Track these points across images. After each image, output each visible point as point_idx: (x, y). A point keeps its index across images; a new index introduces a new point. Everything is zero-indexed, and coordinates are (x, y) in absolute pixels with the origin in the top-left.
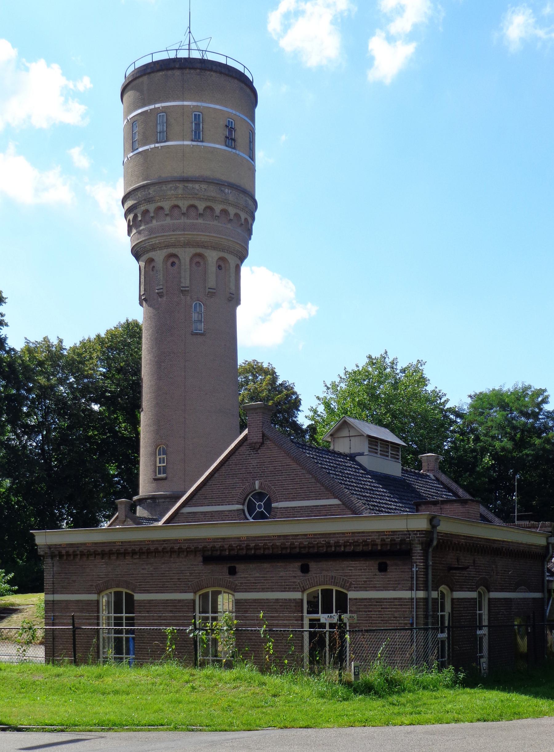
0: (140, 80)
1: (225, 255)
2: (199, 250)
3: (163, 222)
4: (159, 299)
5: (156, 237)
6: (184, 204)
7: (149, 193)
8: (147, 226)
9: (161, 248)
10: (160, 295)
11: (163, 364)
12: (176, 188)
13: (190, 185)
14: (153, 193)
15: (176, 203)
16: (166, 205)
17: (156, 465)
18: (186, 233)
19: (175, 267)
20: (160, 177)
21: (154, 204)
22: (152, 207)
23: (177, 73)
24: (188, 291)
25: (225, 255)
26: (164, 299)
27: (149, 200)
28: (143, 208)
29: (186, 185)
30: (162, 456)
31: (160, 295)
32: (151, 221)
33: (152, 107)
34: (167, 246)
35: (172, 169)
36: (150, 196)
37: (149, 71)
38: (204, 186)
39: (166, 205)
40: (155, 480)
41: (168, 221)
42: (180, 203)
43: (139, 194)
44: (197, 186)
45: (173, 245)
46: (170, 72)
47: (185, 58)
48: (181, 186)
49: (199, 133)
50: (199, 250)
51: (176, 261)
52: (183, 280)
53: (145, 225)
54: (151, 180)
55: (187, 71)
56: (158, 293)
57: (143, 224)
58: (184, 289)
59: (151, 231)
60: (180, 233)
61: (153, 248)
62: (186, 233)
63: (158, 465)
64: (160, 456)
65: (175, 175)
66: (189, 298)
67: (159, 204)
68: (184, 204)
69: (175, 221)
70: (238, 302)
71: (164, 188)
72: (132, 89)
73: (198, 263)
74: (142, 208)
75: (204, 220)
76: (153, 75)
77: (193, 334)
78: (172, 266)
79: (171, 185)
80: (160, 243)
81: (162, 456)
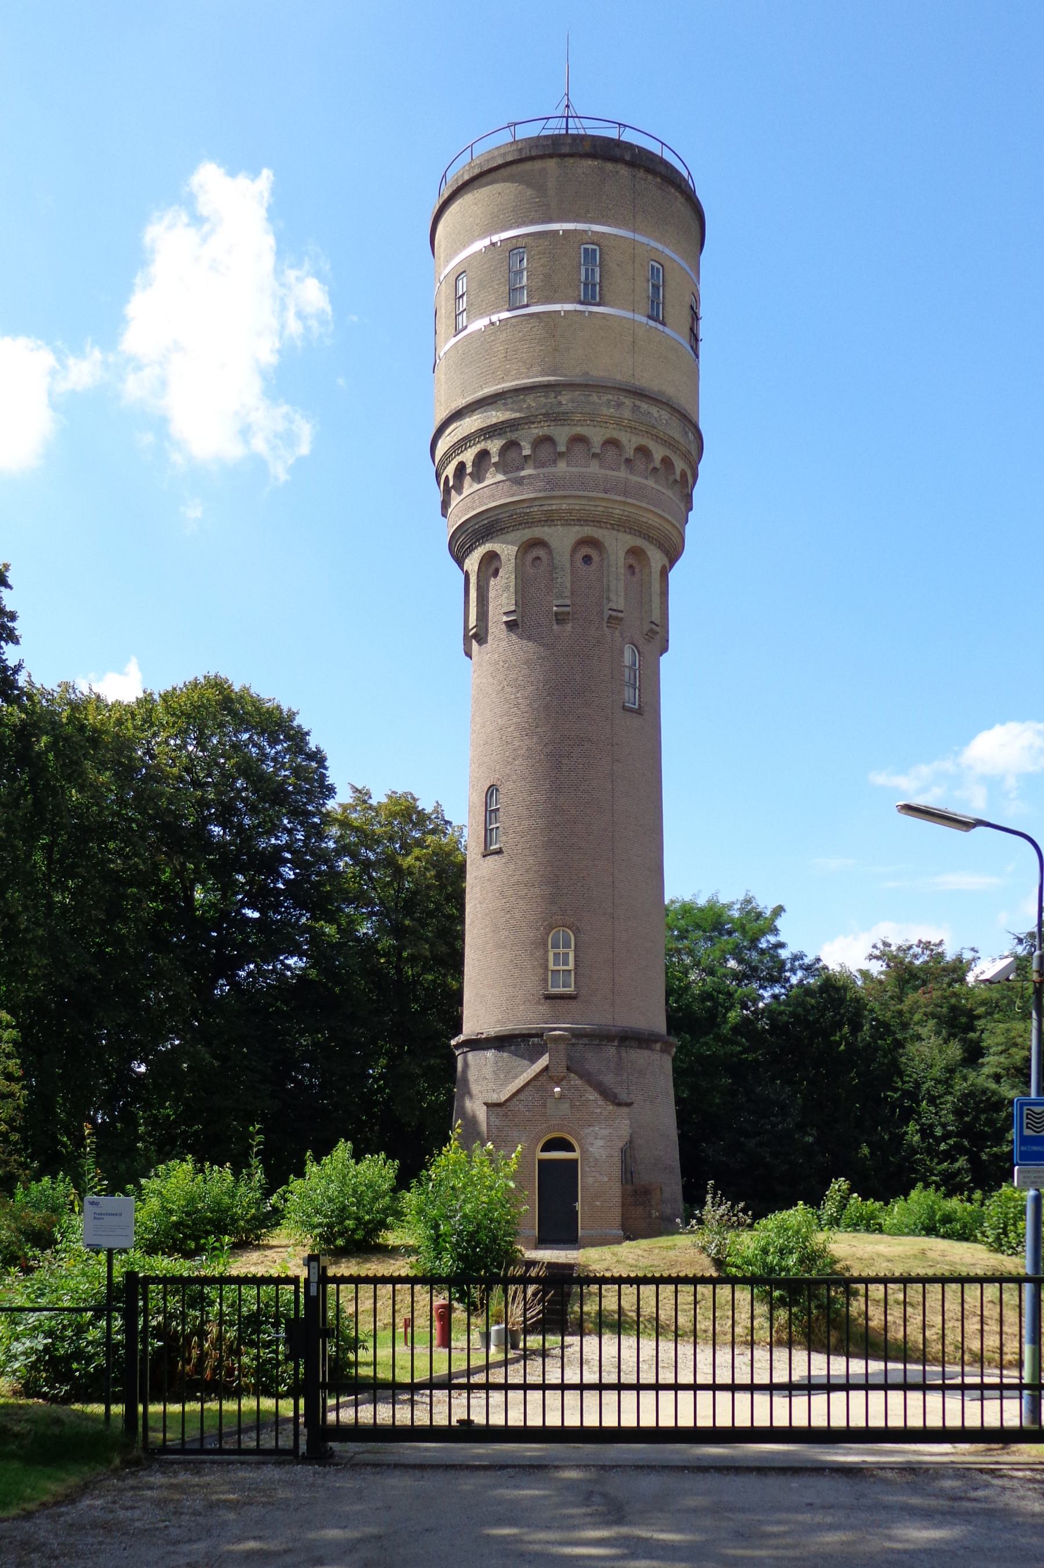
0: (538, 165)
1: (538, 532)
2: (588, 531)
3: (583, 470)
4: (555, 627)
5: (565, 497)
6: (630, 442)
7: (560, 404)
8: (541, 470)
9: (567, 523)
10: (560, 619)
11: (565, 761)
12: (619, 405)
13: (644, 406)
14: (570, 405)
15: (615, 434)
16: (597, 436)
17: (547, 967)
18: (629, 500)
19: (594, 566)
20: (587, 373)
21: (567, 428)
22: (562, 434)
23: (624, 171)
24: (621, 619)
25: (538, 532)
26: (569, 627)
27: (558, 418)
28: (537, 431)
29: (638, 403)
30: (561, 950)
31: (560, 619)
32: (555, 462)
33: (580, 226)
34: (582, 521)
35: (610, 364)
36: (562, 409)
37: (565, 150)
38: (665, 415)
39: (597, 436)
40: (549, 997)
41: (594, 468)
42: (624, 437)
43: (530, 401)
44: (654, 411)
45: (597, 522)
46: (609, 166)
47: (613, 140)
48: (628, 402)
49: (658, 304)
50: (588, 531)
51: (594, 554)
52: (612, 596)
53: (535, 467)
54: (565, 376)
55: (641, 174)
56: (556, 614)
57: (531, 462)
58: (614, 613)
59: (552, 483)
60: (618, 498)
61: (549, 519)
62: (629, 500)
63: (551, 967)
64: (556, 950)
65: (619, 377)
66: (617, 634)
67: (579, 430)
68: (630, 442)
69: (608, 472)
70: (665, 649)
71: (594, 398)
72: (525, 180)
73: (587, 559)
74: (536, 431)
75: (656, 482)
76: (571, 160)
77: (624, 708)
78: (585, 562)
79: (610, 397)
80: (570, 512)
81: (561, 950)
